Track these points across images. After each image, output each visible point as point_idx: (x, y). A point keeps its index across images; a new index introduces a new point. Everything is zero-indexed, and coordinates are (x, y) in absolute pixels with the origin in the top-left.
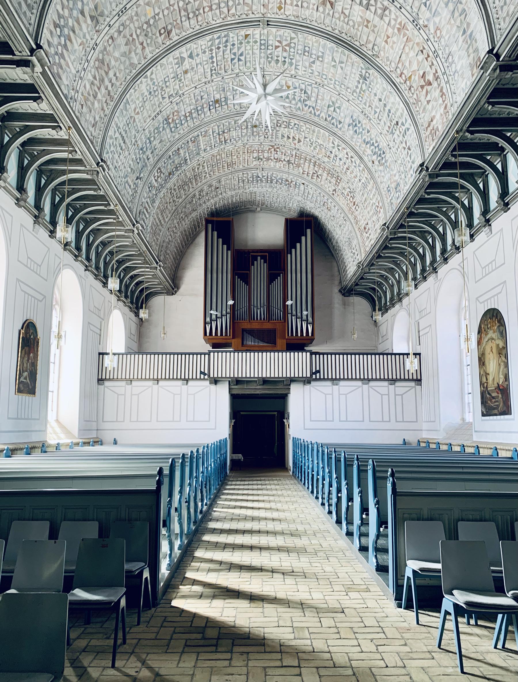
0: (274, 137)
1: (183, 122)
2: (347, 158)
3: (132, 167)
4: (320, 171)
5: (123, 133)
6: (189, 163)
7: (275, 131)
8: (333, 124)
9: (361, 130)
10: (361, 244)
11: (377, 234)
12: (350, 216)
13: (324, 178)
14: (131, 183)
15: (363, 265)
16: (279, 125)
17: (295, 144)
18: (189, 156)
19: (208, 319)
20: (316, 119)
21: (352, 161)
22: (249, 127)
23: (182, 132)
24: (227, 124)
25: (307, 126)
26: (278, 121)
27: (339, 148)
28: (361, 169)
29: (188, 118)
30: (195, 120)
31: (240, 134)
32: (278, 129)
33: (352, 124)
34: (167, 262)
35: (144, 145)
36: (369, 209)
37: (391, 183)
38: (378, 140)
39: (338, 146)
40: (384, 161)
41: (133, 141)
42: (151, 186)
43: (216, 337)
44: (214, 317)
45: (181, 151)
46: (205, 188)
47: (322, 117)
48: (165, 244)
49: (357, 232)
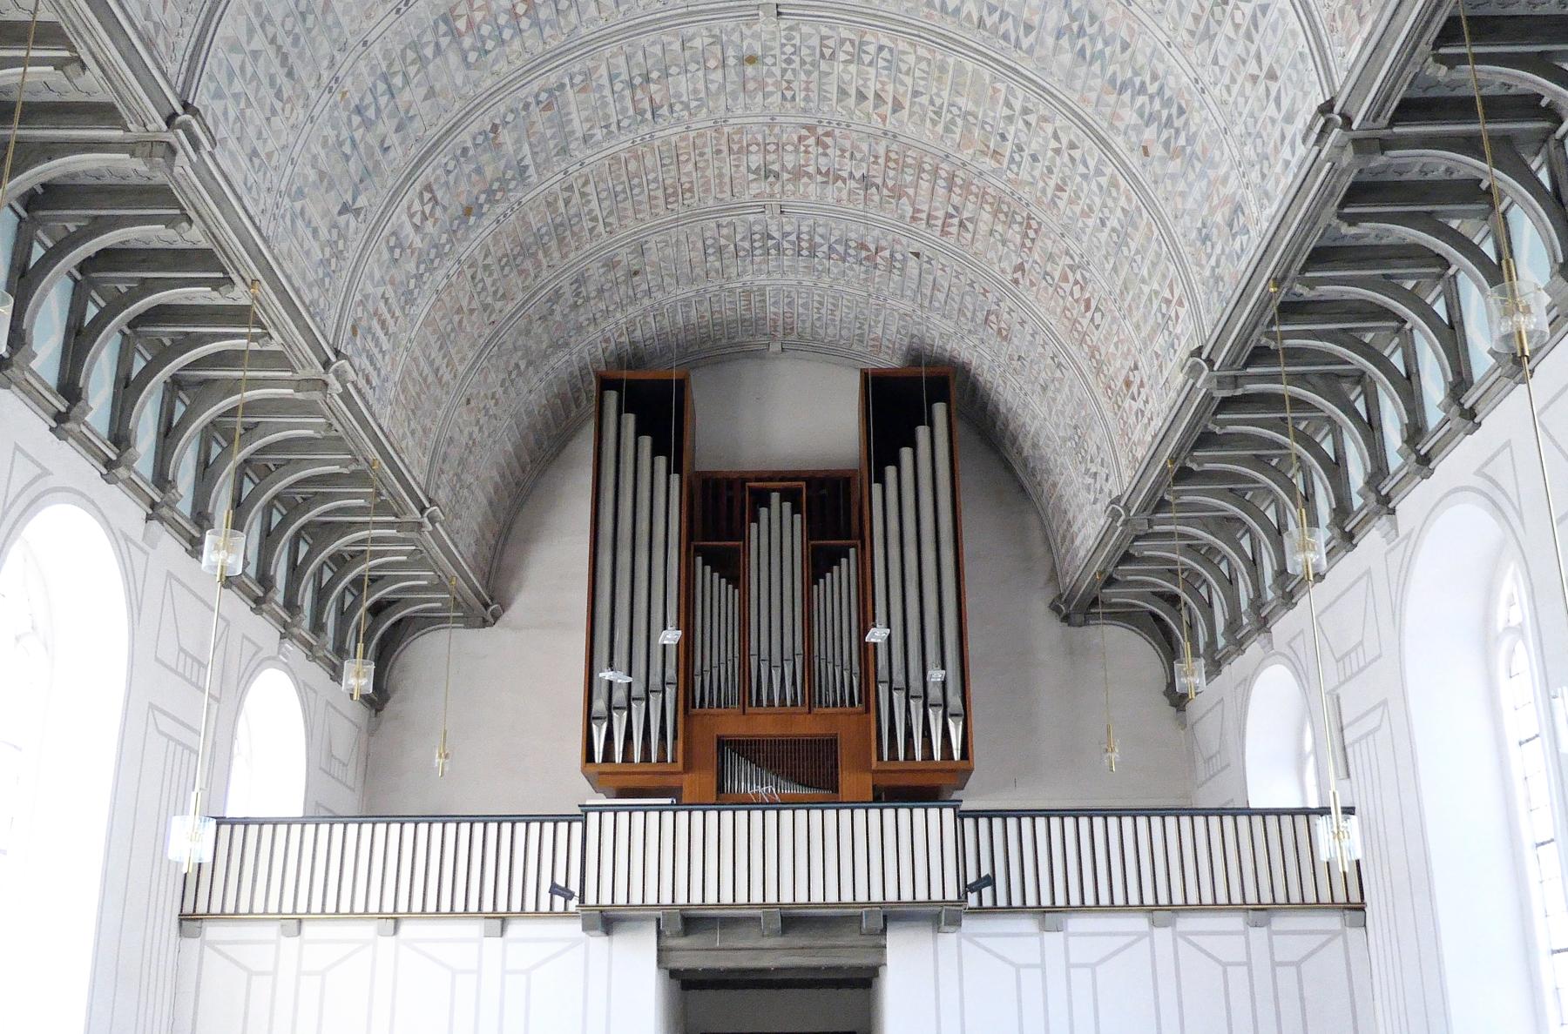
0: (814, 96)
1: (507, 34)
2: (1057, 151)
3: (323, 163)
4: (970, 206)
5: (286, 43)
6: (534, 179)
7: (816, 74)
8: (1005, 37)
9: (1100, 45)
10: (1116, 439)
11: (1173, 394)
12: (1073, 349)
13: (983, 228)
14: (317, 221)
15: (1127, 508)
16: (827, 52)
17: (884, 119)
18: (534, 154)
19: (600, 705)
20: (949, 26)
21: (1072, 159)
22: (731, 61)
23: (502, 67)
24: (657, 49)
25: (922, 52)
26: (823, 38)
27: (1032, 119)
28: (1104, 181)
29: (525, 23)
30: (547, 31)
31: (701, 86)
32: (824, 66)
33: (1069, 27)
34: (465, 513)
35: (369, 99)
37: (1212, 211)
38: (1160, 69)
39: (1026, 111)
40: (1182, 141)
41: (326, 76)
42: (398, 244)
43: (627, 768)
44: (619, 696)
45: (506, 137)
46: (596, 270)
47: (969, 14)
48: (454, 453)
49: (1103, 400)
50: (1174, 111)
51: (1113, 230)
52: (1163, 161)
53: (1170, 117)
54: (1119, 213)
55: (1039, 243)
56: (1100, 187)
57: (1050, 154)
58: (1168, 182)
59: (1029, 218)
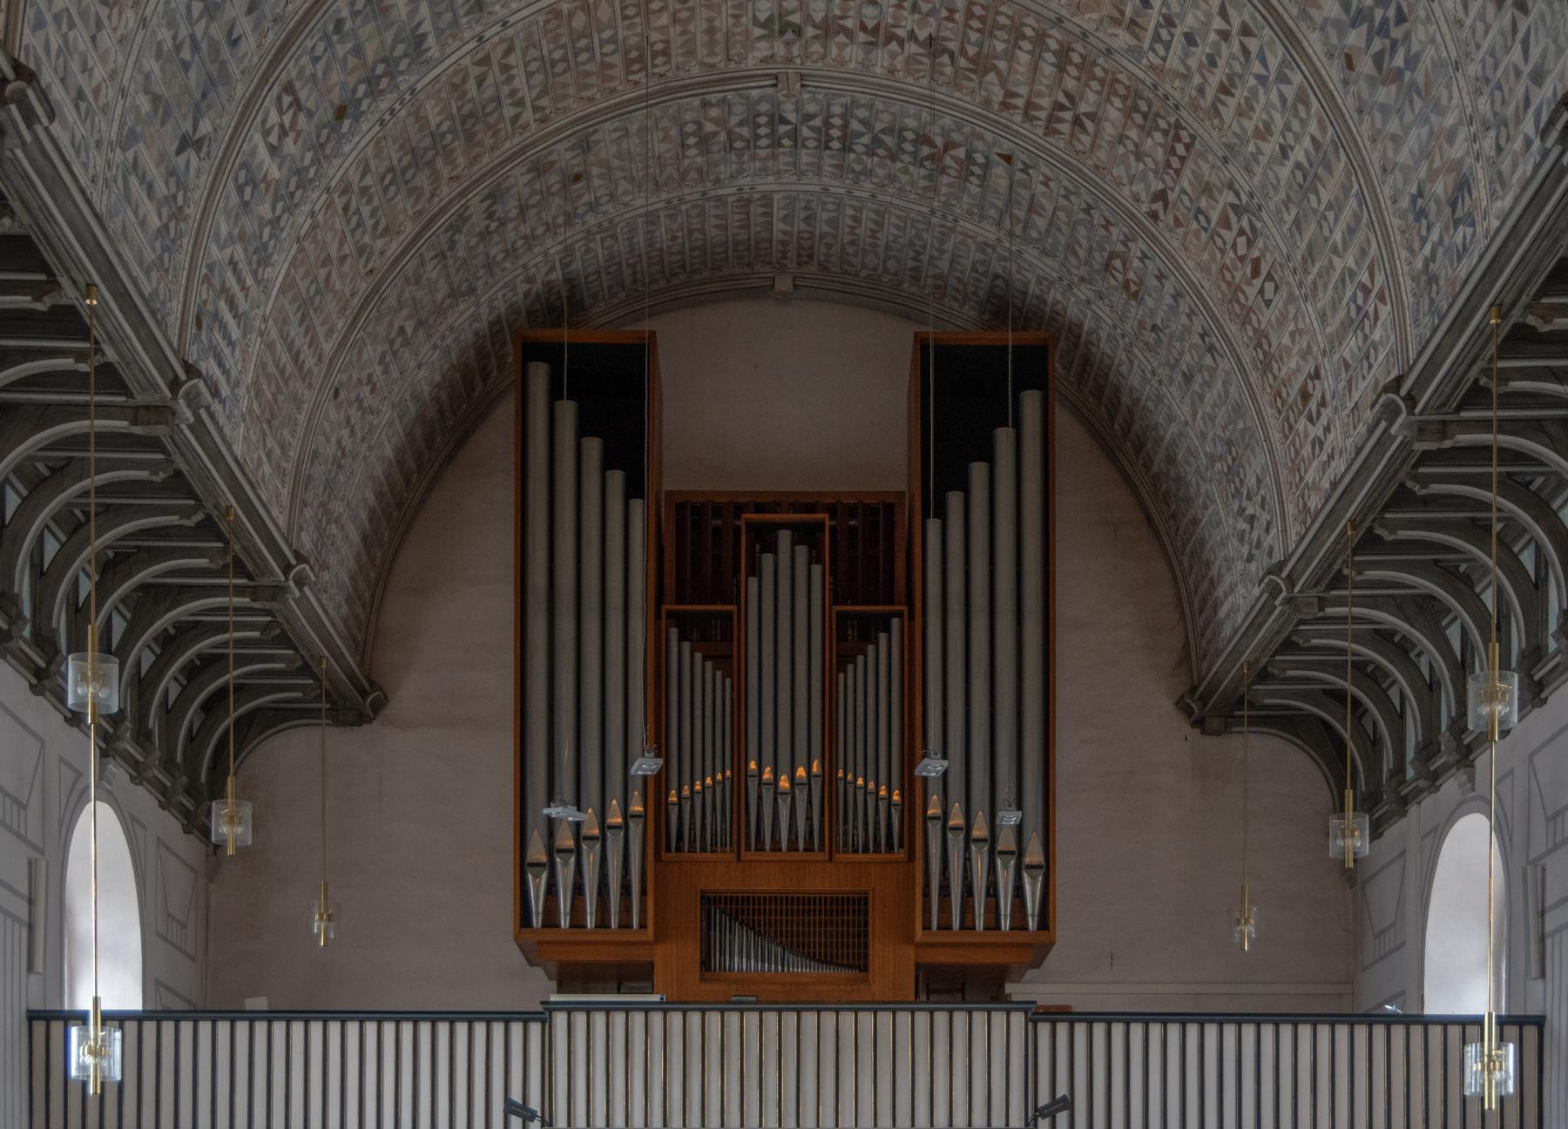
2: (1224, 35)
12: (1232, 329)
21: (1245, 51)
28: (1289, 92)
36: (1324, 300)
40: (1399, 61)
49: (1269, 412)
50: (1392, 13)
51: (1298, 166)
52: (1372, 83)
53: (1385, 20)
54: (1307, 142)
55: (1190, 164)
56: (1283, 100)
57: (1213, 37)
58: (1378, 116)
59: (1178, 126)
